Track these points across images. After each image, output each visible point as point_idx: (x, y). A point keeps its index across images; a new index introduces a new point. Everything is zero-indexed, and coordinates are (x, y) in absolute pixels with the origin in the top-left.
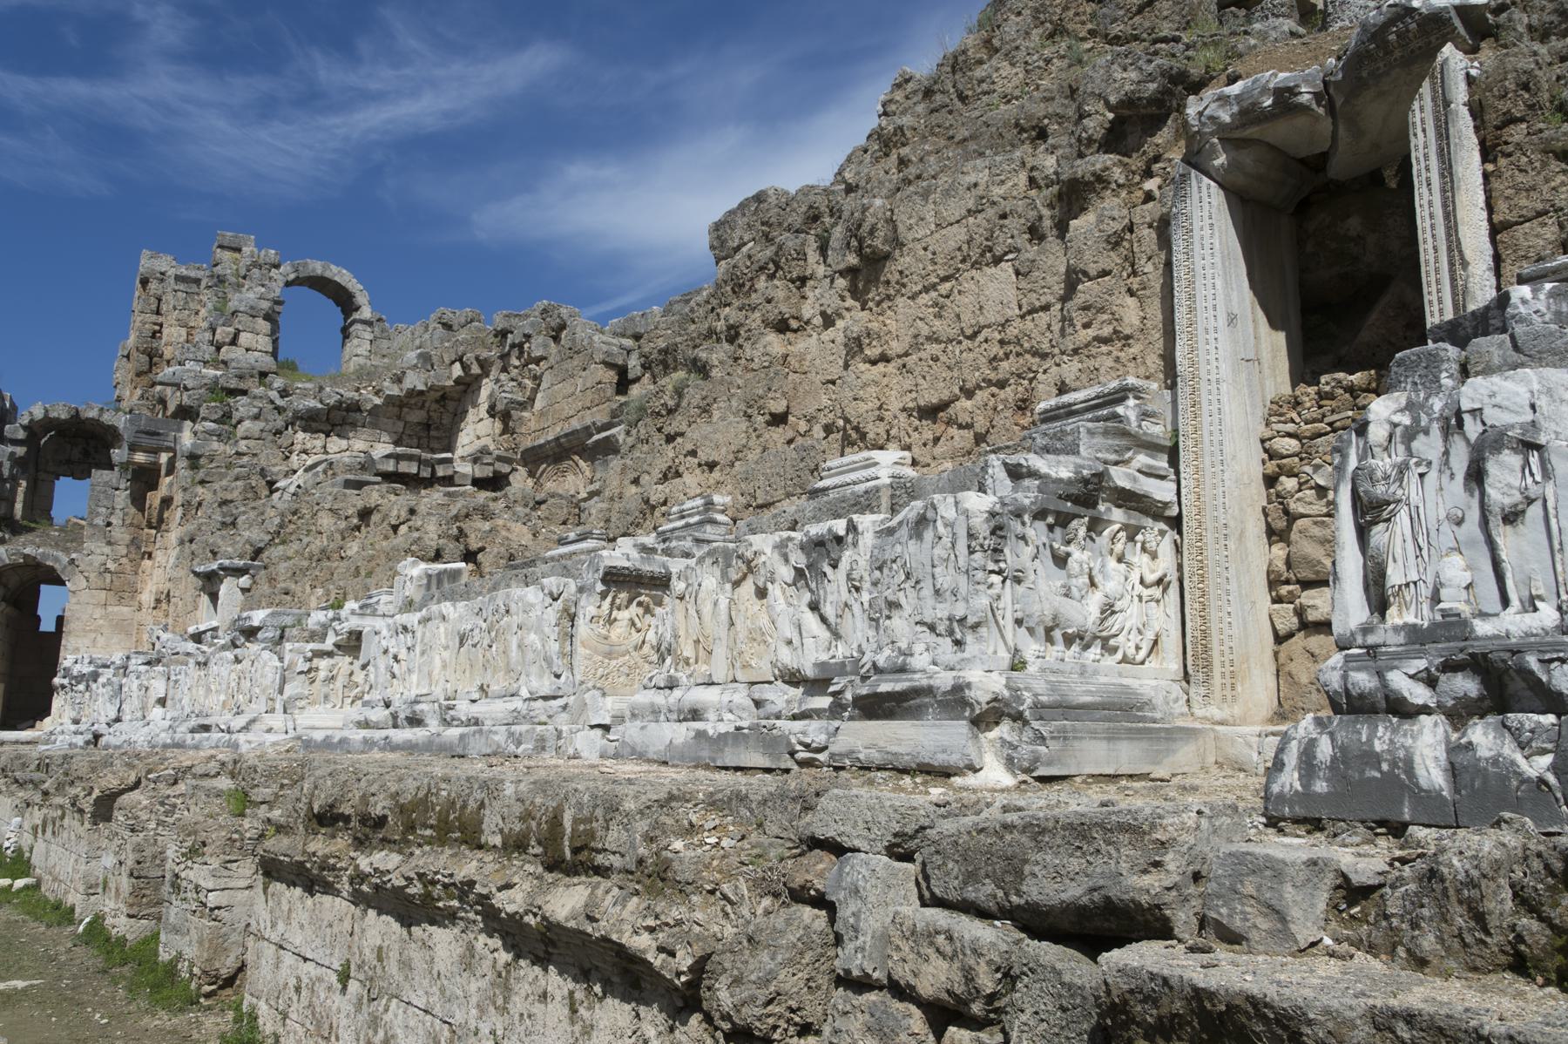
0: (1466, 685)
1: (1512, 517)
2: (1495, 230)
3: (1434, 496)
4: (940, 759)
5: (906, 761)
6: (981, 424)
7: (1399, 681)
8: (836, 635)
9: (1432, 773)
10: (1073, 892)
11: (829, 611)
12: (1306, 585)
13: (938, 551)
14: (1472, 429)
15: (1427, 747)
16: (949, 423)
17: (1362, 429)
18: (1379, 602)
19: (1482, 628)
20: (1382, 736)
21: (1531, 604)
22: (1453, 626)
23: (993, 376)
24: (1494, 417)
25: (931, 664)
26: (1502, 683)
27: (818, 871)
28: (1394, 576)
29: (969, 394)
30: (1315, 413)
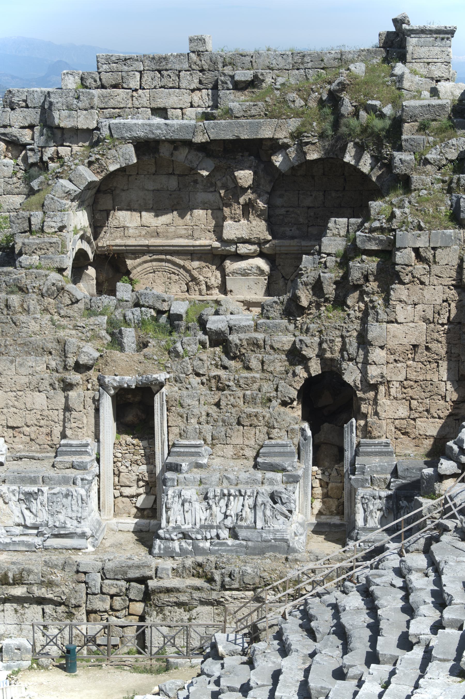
0: (181, 536)
1: (187, 512)
2: (168, 427)
3: (176, 507)
4: (79, 547)
5: (69, 547)
6: (33, 436)
7: (173, 536)
8: (36, 516)
9: (178, 550)
10: (137, 575)
11: (34, 510)
12: (122, 486)
13: (73, 502)
14: (183, 498)
15: (176, 545)
16: (20, 432)
17: (167, 495)
18: (168, 522)
19: (183, 527)
20: (171, 544)
21: (188, 524)
22: (179, 527)
23: (38, 424)
24: (186, 497)
25: (71, 526)
26: (185, 536)
27: (82, 577)
28: (171, 519)
29: (28, 426)
30: (125, 448)
